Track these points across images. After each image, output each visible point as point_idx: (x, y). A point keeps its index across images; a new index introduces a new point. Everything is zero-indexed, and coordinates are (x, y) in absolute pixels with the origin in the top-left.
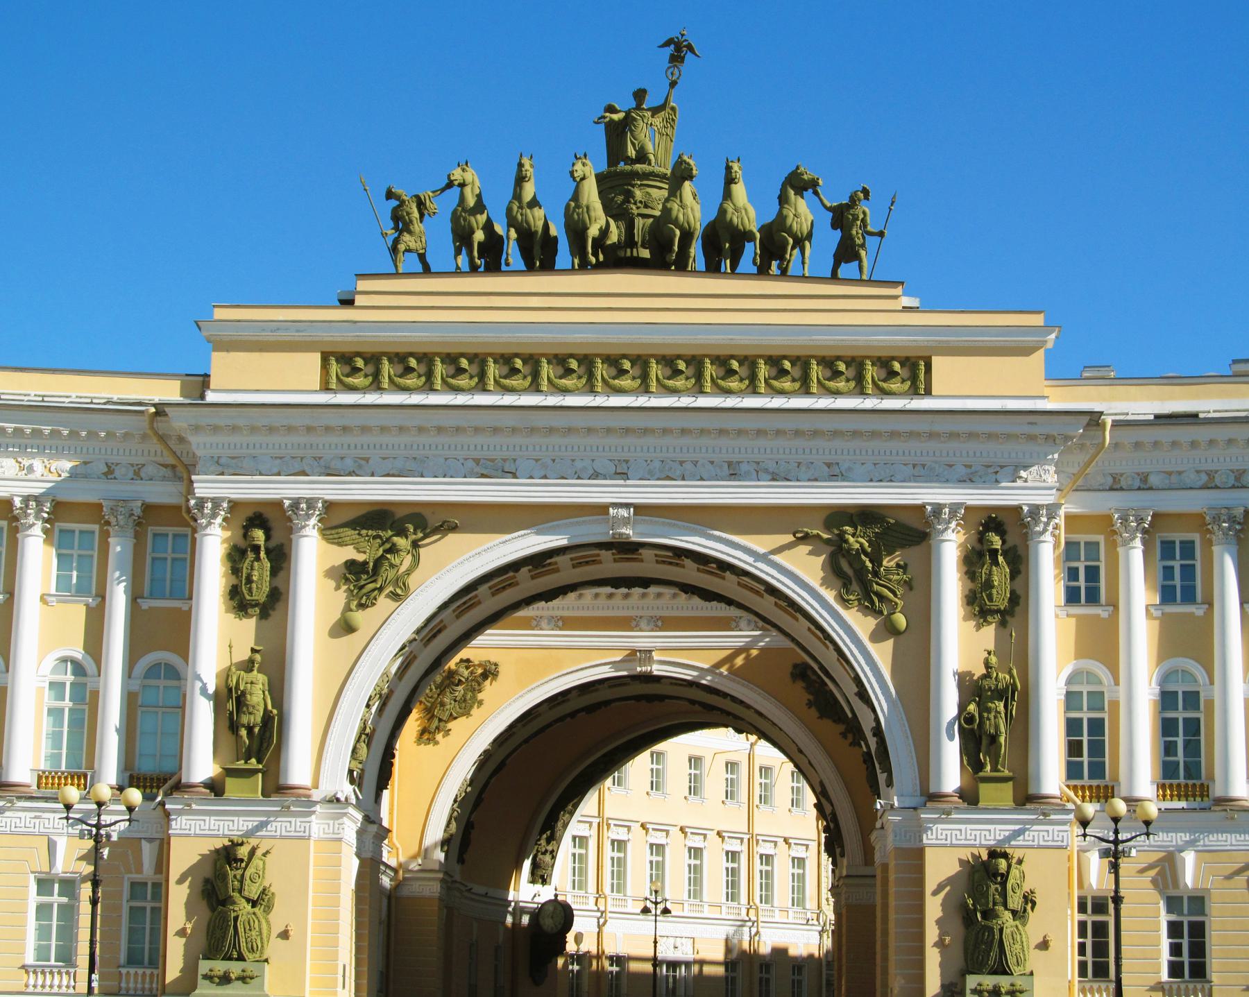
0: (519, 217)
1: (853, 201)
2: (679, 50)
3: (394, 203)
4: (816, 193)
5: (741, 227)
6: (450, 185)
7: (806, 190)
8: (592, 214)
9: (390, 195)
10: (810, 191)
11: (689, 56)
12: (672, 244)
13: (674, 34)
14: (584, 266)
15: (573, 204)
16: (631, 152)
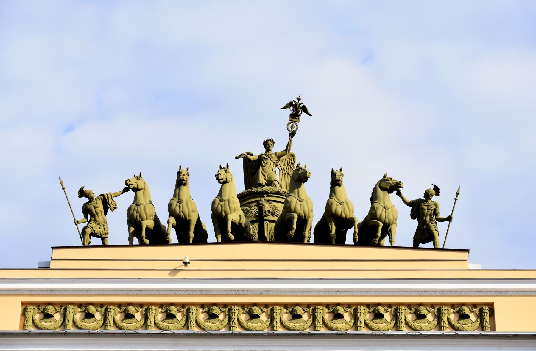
0: (178, 209)
1: (427, 195)
2: (297, 110)
3: (85, 200)
4: (399, 194)
5: (343, 215)
6: (126, 190)
7: (390, 191)
8: (232, 206)
9: (82, 193)
10: (395, 192)
11: (303, 115)
12: (292, 223)
13: (293, 99)
14: (226, 240)
15: (218, 200)
16: (262, 180)
